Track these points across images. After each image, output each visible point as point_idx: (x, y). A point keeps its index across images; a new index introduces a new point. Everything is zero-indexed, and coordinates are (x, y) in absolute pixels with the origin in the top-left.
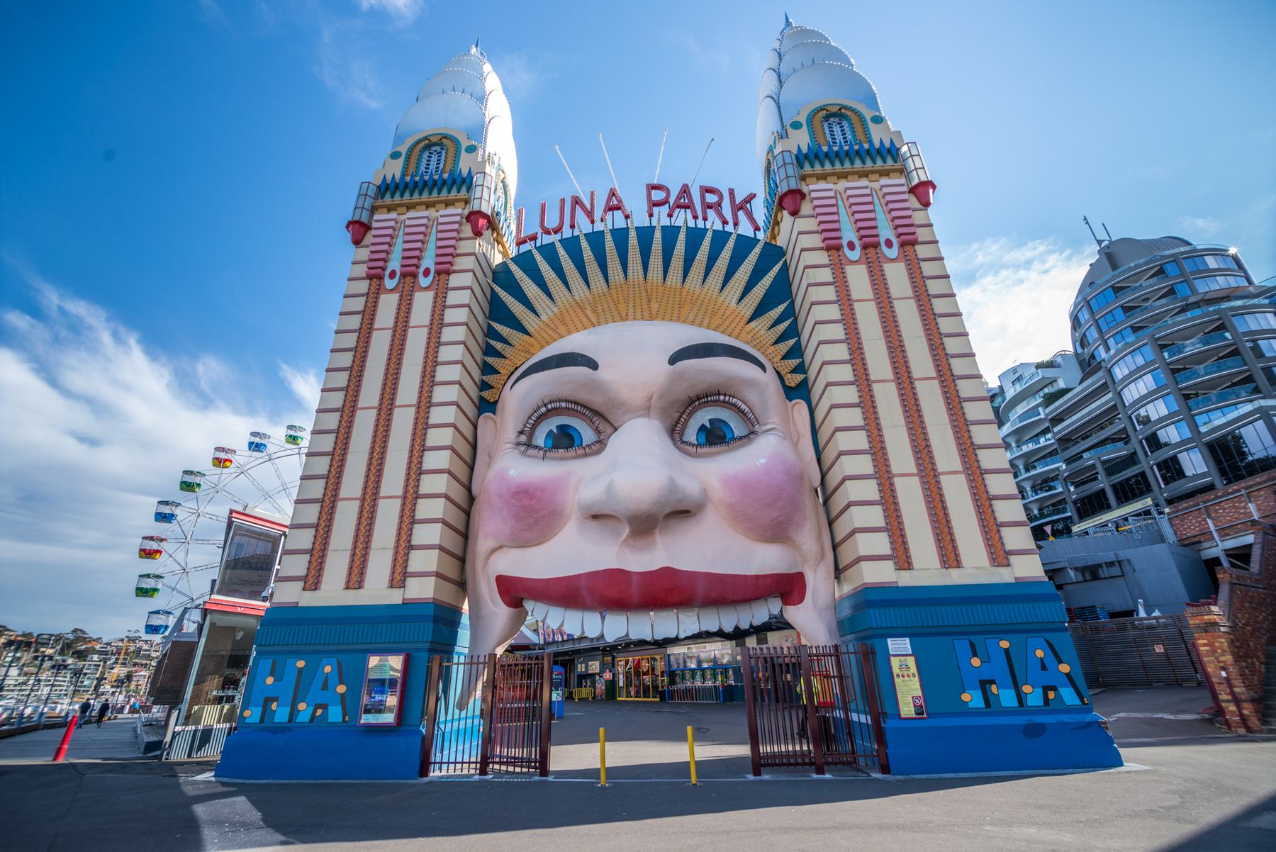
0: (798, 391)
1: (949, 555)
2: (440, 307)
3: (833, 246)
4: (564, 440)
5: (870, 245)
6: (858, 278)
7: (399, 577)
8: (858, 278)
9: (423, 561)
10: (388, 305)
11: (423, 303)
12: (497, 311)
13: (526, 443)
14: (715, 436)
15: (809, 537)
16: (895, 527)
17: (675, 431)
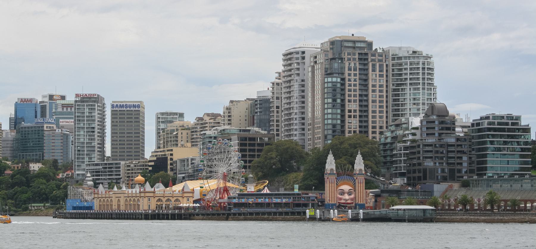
0: (355, 191)
1: (361, 202)
2: (334, 185)
3: (358, 183)
4: (342, 194)
5: (361, 183)
6: (359, 185)
7: (334, 202)
8: (359, 185)
9: (335, 201)
10: (331, 184)
11: (333, 184)
12: (337, 184)
13: (339, 194)
14: (350, 195)
15: (354, 200)
16: (358, 201)
17: (348, 194)
